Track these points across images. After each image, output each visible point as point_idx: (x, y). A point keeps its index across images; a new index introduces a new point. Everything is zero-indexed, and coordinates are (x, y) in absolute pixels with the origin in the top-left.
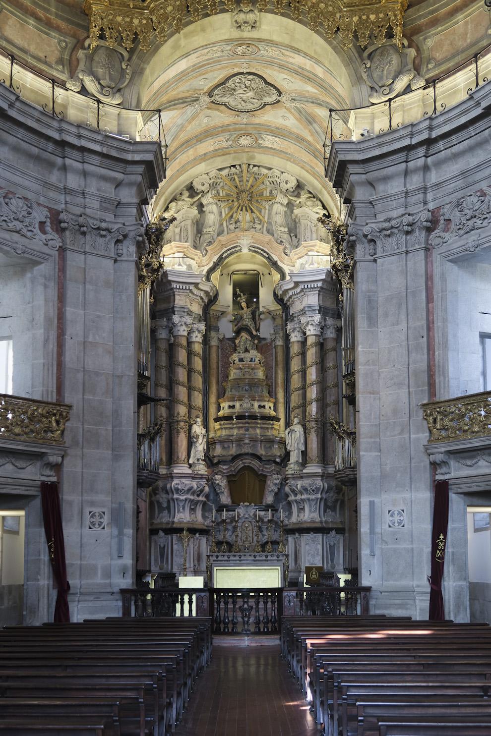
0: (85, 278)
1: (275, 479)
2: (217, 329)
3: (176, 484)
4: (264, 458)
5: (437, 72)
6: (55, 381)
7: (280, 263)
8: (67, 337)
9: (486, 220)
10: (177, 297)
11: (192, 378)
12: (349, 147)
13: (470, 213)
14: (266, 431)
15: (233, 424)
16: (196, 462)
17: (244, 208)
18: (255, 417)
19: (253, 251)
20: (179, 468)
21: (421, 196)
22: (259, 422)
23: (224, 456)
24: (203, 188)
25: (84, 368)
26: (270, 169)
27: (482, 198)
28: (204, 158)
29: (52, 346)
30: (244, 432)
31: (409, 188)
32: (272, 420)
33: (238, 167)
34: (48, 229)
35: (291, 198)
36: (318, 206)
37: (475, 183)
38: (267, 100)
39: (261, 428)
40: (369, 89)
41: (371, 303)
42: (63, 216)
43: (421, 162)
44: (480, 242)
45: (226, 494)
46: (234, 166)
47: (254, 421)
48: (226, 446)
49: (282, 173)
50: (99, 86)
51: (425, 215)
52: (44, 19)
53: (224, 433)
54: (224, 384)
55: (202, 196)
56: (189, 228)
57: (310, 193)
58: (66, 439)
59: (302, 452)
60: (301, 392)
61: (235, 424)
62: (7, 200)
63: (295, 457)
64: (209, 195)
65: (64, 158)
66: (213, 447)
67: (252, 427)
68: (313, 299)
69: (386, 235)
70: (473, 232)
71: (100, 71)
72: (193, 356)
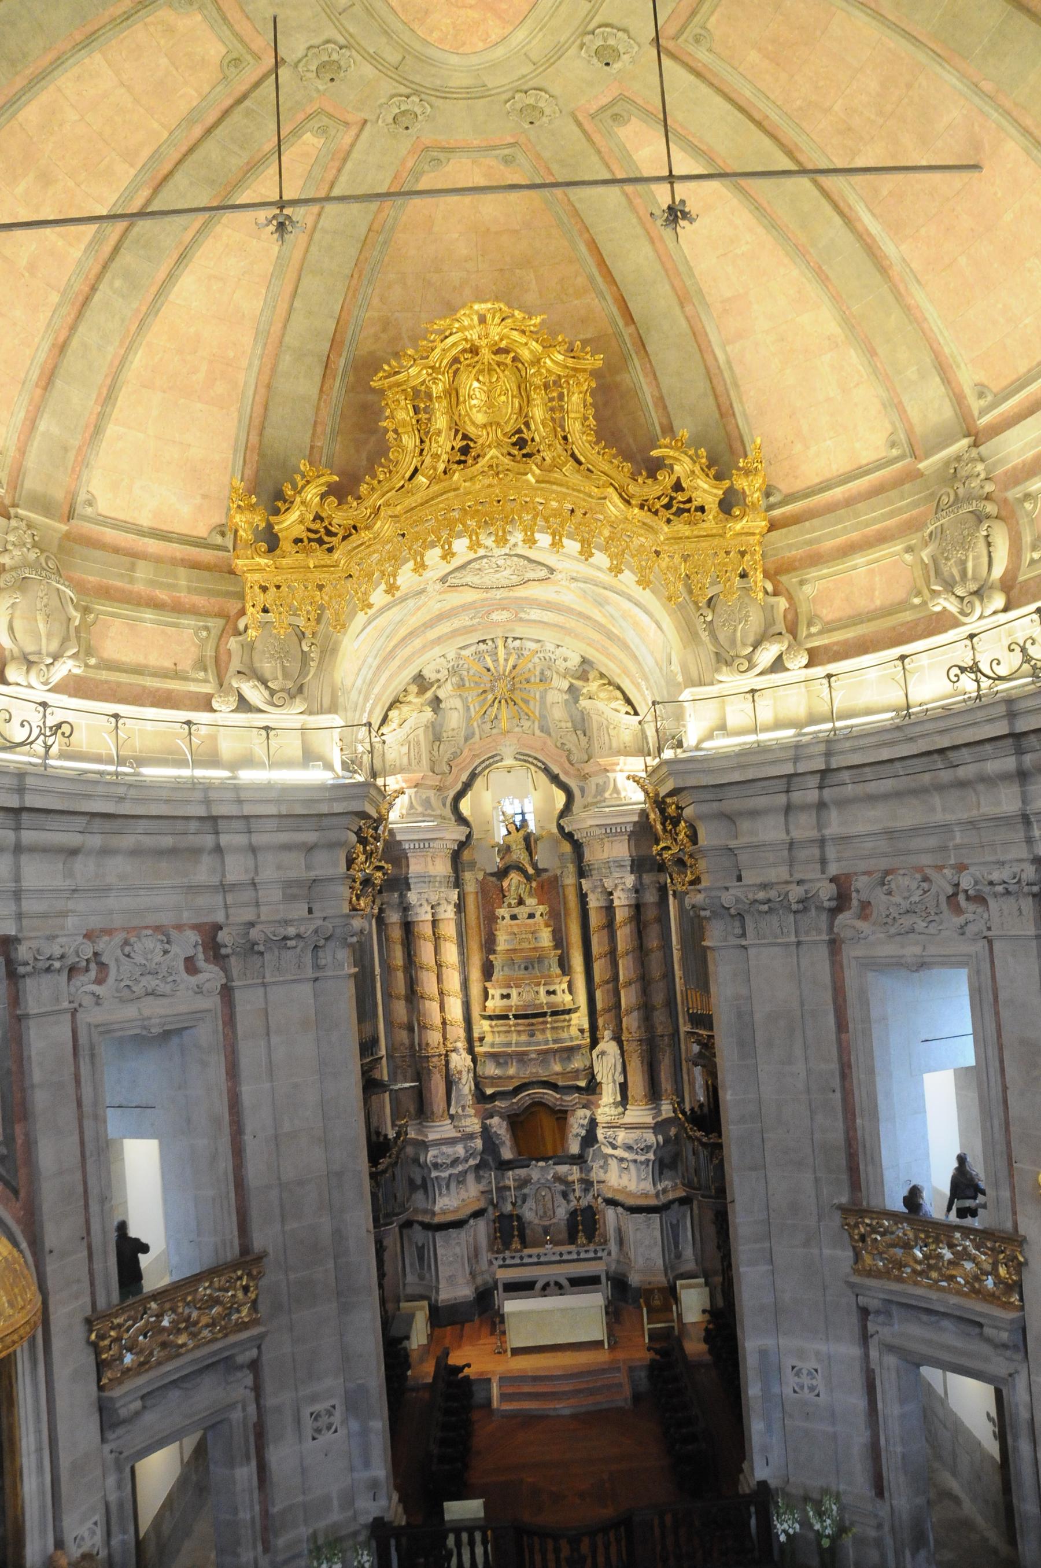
0: (268, 1027)
2: (472, 865)
5: (826, 642)
6: (234, 1218)
7: (563, 777)
8: (248, 1138)
9: (933, 924)
10: (412, 861)
11: (444, 977)
12: (690, 766)
13: (905, 905)
16: (460, 1110)
17: (503, 701)
18: (544, 1014)
19: (520, 760)
20: (436, 1129)
21: (816, 852)
22: (549, 1019)
24: (439, 676)
25: (279, 1179)
26: (539, 641)
27: (925, 885)
28: (439, 641)
29: (225, 1164)
31: (796, 834)
33: (490, 643)
34: (201, 964)
35: (573, 681)
36: (617, 699)
37: (909, 852)
38: (531, 575)
39: (553, 1028)
40: (712, 656)
41: (744, 1019)
42: (222, 936)
43: (813, 796)
44: (927, 960)
45: (508, 1143)
46: (484, 641)
47: (541, 1020)
48: (501, 1061)
49: (558, 646)
50: (266, 693)
51: (826, 891)
52: (169, 601)
53: (498, 1039)
54: (491, 957)
55: (439, 687)
56: (422, 738)
57: (602, 676)
58: (263, 1308)
59: (620, 1084)
60: (610, 986)
61: (515, 1025)
62: (127, 949)
63: (609, 1095)
64: (449, 686)
65: (217, 833)
68: (621, 850)
69: (760, 912)
70: (911, 935)
71: (267, 667)
72: (442, 942)
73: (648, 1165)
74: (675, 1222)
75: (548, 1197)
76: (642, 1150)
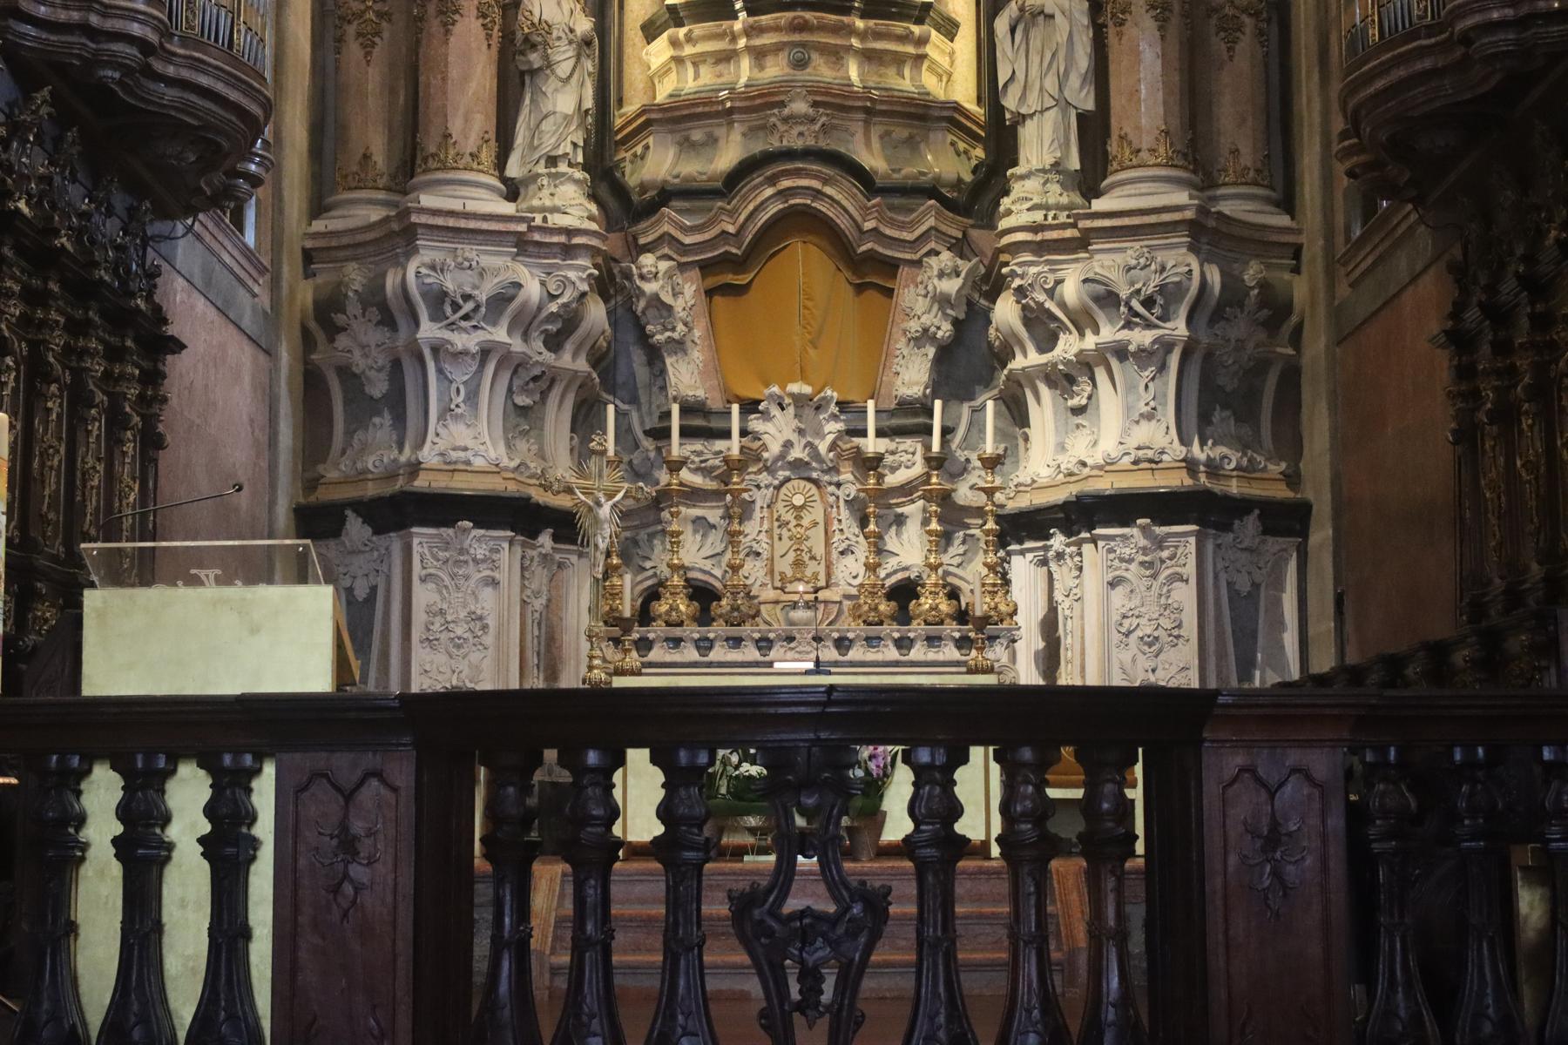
1: (941, 275)
3: (433, 267)
4: (879, 182)
14: (891, 71)
15: (734, 39)
20: (449, 189)
22: (860, 24)
23: (687, 179)
30: (787, 70)
32: (920, 21)
39: (869, 56)
61: (749, 32)
66: (639, 149)
67: (824, 50)
73: (1162, 368)
74: (1244, 585)
75: (817, 513)
76: (1148, 303)
